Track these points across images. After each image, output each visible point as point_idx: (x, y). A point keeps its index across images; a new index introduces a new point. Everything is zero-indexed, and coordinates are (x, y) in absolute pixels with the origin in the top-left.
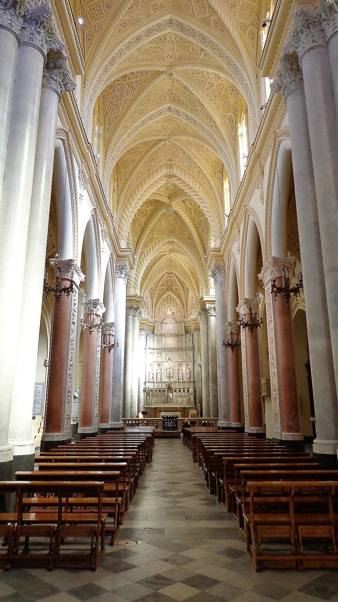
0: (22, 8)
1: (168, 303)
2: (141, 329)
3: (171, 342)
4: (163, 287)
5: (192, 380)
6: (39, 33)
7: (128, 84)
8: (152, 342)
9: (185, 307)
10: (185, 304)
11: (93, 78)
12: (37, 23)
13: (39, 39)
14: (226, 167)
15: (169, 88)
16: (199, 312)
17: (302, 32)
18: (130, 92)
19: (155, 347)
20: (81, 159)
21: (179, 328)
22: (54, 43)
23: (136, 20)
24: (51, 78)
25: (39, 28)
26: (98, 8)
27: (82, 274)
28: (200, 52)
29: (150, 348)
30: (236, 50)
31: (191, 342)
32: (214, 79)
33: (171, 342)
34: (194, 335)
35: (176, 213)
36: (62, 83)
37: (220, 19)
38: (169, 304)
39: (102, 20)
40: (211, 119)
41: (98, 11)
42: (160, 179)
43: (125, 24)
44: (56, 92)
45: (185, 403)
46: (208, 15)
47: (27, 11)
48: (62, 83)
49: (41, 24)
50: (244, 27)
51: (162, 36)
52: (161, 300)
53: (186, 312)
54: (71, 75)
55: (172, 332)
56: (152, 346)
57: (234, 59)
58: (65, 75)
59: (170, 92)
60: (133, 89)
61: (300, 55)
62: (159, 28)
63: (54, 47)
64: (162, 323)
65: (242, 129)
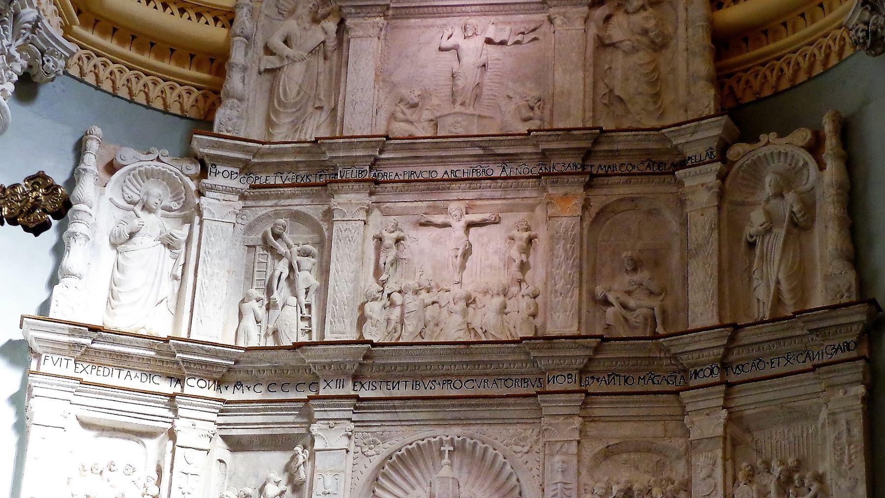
3: (469, 265)
8: (150, 262)
21: (626, 71)
31: (827, 239)
33: (469, 265)
56: (145, 311)
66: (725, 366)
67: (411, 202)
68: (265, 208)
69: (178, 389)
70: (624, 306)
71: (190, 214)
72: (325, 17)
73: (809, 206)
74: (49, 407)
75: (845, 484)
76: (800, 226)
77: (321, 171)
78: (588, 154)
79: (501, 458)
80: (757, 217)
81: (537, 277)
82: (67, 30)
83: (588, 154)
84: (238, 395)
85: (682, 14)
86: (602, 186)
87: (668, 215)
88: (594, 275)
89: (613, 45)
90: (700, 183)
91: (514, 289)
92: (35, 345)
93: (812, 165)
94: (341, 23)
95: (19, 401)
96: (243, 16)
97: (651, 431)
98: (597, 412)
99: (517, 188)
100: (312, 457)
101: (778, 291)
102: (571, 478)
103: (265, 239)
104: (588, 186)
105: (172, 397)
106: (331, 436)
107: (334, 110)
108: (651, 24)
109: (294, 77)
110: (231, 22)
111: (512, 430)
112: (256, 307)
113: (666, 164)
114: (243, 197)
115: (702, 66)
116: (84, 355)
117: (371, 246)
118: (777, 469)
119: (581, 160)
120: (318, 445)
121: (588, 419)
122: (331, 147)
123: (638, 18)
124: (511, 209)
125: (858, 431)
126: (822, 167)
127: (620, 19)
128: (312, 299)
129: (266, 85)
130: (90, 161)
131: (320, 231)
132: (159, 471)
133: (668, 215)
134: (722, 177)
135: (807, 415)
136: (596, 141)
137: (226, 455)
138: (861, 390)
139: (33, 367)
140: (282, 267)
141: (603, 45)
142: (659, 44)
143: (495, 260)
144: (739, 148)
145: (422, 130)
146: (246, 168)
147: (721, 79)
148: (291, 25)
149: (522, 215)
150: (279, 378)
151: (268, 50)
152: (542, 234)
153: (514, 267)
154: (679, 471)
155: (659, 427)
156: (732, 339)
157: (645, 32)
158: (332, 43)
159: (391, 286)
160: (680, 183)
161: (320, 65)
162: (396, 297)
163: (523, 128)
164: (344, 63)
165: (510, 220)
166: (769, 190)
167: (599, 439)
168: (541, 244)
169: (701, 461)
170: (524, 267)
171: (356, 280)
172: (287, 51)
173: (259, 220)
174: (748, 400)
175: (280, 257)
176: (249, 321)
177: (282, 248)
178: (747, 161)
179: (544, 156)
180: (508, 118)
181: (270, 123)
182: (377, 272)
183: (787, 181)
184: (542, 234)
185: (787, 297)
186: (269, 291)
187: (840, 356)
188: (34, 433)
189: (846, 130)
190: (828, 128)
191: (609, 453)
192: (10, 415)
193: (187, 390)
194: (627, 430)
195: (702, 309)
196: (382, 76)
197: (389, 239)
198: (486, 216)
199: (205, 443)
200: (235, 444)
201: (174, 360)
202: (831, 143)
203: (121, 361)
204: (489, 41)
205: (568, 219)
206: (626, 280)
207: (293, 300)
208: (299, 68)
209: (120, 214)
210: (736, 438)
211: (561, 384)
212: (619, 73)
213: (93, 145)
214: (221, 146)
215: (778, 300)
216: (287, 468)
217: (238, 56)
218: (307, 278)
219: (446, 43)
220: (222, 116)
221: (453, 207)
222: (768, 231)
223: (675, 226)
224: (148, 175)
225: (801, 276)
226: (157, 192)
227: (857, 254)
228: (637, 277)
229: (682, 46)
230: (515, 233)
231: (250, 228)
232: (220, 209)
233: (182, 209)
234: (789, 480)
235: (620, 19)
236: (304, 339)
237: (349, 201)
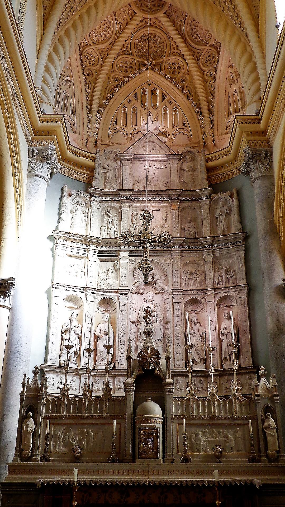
2: (38, 156)
4: (127, 58)
5: (246, 361)
8: (80, 217)
10: (204, 104)
19: (95, 233)
21: (187, 176)
31: (235, 217)
34: (246, 192)
45: (237, 458)
52: (121, 95)
53: (207, 127)
55: (160, 186)
56: (80, 228)
64: (120, 157)
66: (212, 245)
67: (138, 205)
68: (105, 205)
69: (88, 247)
70: (189, 230)
71: (89, 206)
72: (117, 160)
73: (230, 210)
74: (60, 251)
75: (240, 273)
76: (228, 214)
77: (119, 197)
78: (179, 195)
79: (162, 265)
80: (218, 212)
81: (169, 223)
82: (59, 161)
83: (179, 195)
84: (102, 249)
85: (199, 163)
86: (184, 203)
87: (197, 210)
88: (181, 224)
89: (184, 170)
90: (205, 203)
91: (164, 226)
92: (56, 237)
93: (231, 200)
94: (121, 162)
95: (53, 249)
96: (97, 159)
97: (196, 259)
98: (183, 255)
99: (163, 203)
100: (120, 263)
101: (224, 228)
102: (179, 269)
103: (105, 212)
104: (180, 203)
105: (87, 249)
106: (124, 259)
107: (120, 182)
108: (192, 165)
109: (110, 174)
110: (95, 160)
111: (164, 258)
112: (104, 228)
113: (197, 198)
114: (100, 203)
115: (205, 176)
116: (67, 239)
117: (130, 215)
118: (225, 269)
119: (178, 197)
120: (121, 261)
121: (182, 256)
122: (121, 192)
123: (189, 164)
124: (162, 207)
125: (243, 261)
126: (233, 201)
127: (185, 163)
128: (117, 227)
129: (103, 176)
130: (66, 193)
131: (118, 211)
132: (85, 266)
133: (197, 210)
134: (210, 202)
135: (231, 257)
136: (181, 193)
137: (100, 263)
138: (244, 252)
139: (56, 242)
140: (110, 219)
141: (181, 169)
142: (194, 170)
143: (159, 219)
144: (213, 195)
145: (141, 188)
146: (101, 196)
147: (209, 179)
148: (109, 162)
149: (164, 209)
150: (111, 245)
151: (104, 168)
152: (170, 213)
153: (164, 221)
154: (202, 268)
155: (197, 258)
156: (214, 239)
157: (191, 167)
158: (119, 166)
159: (136, 225)
160: (200, 203)
161: (117, 172)
162: (137, 227)
163: (164, 189)
164: (121, 171)
165: (162, 210)
166: (221, 206)
167: (184, 261)
168: (169, 216)
169: (207, 266)
170: (166, 221)
171: (128, 222)
172: (108, 168)
173: (104, 208)
174: (218, 253)
175: (109, 217)
176: (103, 232)
177: (110, 215)
178: (216, 198)
179: (169, 196)
180: (161, 186)
181: (105, 185)
182: (132, 221)
183: (225, 204)
184: (170, 213)
185: (226, 230)
186: (107, 225)
187: (239, 244)
188: (57, 257)
189: (238, 192)
190: (234, 192)
191: (186, 264)
192: (51, 253)
193: (90, 248)
194: (190, 259)
195: (206, 232)
196: (131, 175)
197: (135, 214)
198: (157, 209)
199: (95, 260)
200: (101, 260)
201: (88, 240)
202: (235, 195)
203: (75, 241)
204: (155, 168)
205: (176, 210)
206: (189, 225)
207: (113, 227)
208: (111, 172)
209: (72, 206)
210: (215, 261)
211: (176, 248)
212: (185, 177)
213: (66, 189)
214: (95, 191)
215: (224, 231)
216: (113, 266)
217: (97, 168)
218: (116, 222)
219: (145, 168)
220: (94, 183)
221: (149, 206)
222: (221, 215)
223: (199, 212)
224: (78, 197)
225: (229, 225)
226: (81, 201)
227: (241, 220)
228: (191, 224)
229: (199, 171)
230: (163, 213)
231: (102, 210)
233: (86, 205)
234: (228, 271)
235: (185, 163)
236: (116, 236)
237: (125, 204)
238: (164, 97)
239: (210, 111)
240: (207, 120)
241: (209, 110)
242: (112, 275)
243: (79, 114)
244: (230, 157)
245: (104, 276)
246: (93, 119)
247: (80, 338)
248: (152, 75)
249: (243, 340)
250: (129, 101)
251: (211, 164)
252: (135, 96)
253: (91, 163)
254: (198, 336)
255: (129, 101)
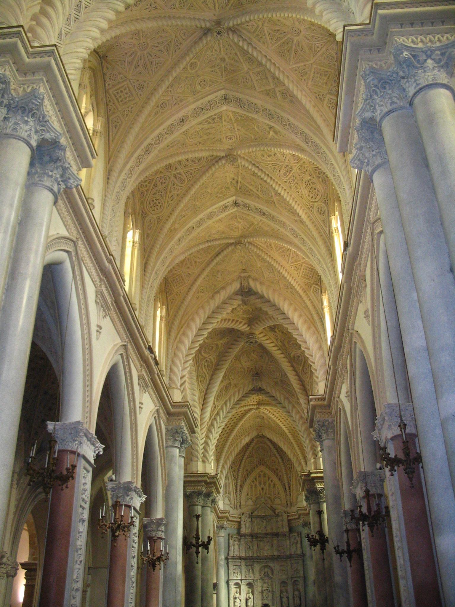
0: (6, 96)
1: (260, 483)
6: (26, 122)
7: (175, 175)
8: (237, 547)
9: (287, 488)
10: (287, 484)
11: (121, 171)
12: (23, 112)
13: (28, 128)
14: (323, 277)
15: (233, 176)
16: (306, 497)
17: (376, 93)
18: (177, 185)
19: (243, 555)
20: (99, 275)
22: (48, 132)
23: (178, 99)
24: (45, 174)
25: (28, 117)
26: (127, 91)
27: (98, 444)
28: (268, 129)
29: (233, 558)
30: (314, 124)
31: (299, 545)
32: (292, 161)
35: (261, 346)
36: (59, 179)
37: (287, 89)
38: (262, 485)
39: (133, 102)
40: (294, 213)
41: (127, 93)
42: (230, 298)
43: (163, 106)
44: (51, 190)
46: (272, 87)
47: (12, 100)
48: (59, 179)
49: (30, 112)
50: (321, 97)
51: (215, 115)
53: (288, 497)
54: (74, 169)
57: (311, 134)
58: (65, 169)
59: (234, 182)
60: (182, 181)
61: (378, 120)
62: (211, 105)
63: (47, 136)
65: (336, 223)
76: (297, 543)
115: (287, 524)
130: (230, 538)
144: (291, 535)
148: (247, 519)
200: (247, 566)
201: (240, 558)
203: (236, 559)
217: (242, 523)
227: (302, 548)
232: (243, 541)
238: (269, 479)
239: (290, 489)
240: (288, 493)
241: (289, 487)
242: (251, 572)
243: (232, 494)
244: (297, 517)
245: (248, 573)
246: (238, 495)
247: (241, 600)
248: (262, 468)
249: (302, 600)
250: (253, 482)
251: (290, 518)
252: (256, 479)
253: (239, 520)
254: (285, 597)
255: (253, 482)
